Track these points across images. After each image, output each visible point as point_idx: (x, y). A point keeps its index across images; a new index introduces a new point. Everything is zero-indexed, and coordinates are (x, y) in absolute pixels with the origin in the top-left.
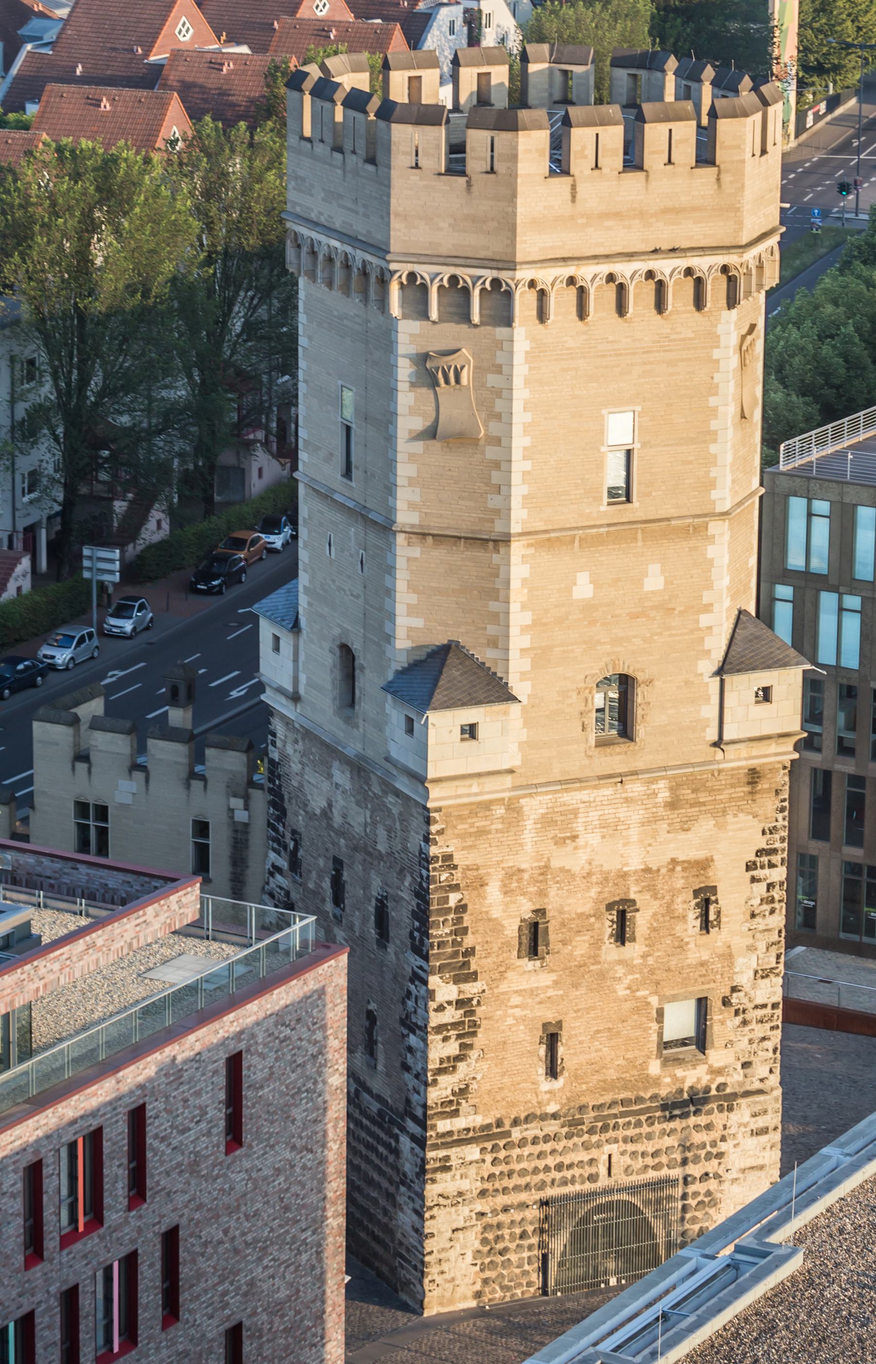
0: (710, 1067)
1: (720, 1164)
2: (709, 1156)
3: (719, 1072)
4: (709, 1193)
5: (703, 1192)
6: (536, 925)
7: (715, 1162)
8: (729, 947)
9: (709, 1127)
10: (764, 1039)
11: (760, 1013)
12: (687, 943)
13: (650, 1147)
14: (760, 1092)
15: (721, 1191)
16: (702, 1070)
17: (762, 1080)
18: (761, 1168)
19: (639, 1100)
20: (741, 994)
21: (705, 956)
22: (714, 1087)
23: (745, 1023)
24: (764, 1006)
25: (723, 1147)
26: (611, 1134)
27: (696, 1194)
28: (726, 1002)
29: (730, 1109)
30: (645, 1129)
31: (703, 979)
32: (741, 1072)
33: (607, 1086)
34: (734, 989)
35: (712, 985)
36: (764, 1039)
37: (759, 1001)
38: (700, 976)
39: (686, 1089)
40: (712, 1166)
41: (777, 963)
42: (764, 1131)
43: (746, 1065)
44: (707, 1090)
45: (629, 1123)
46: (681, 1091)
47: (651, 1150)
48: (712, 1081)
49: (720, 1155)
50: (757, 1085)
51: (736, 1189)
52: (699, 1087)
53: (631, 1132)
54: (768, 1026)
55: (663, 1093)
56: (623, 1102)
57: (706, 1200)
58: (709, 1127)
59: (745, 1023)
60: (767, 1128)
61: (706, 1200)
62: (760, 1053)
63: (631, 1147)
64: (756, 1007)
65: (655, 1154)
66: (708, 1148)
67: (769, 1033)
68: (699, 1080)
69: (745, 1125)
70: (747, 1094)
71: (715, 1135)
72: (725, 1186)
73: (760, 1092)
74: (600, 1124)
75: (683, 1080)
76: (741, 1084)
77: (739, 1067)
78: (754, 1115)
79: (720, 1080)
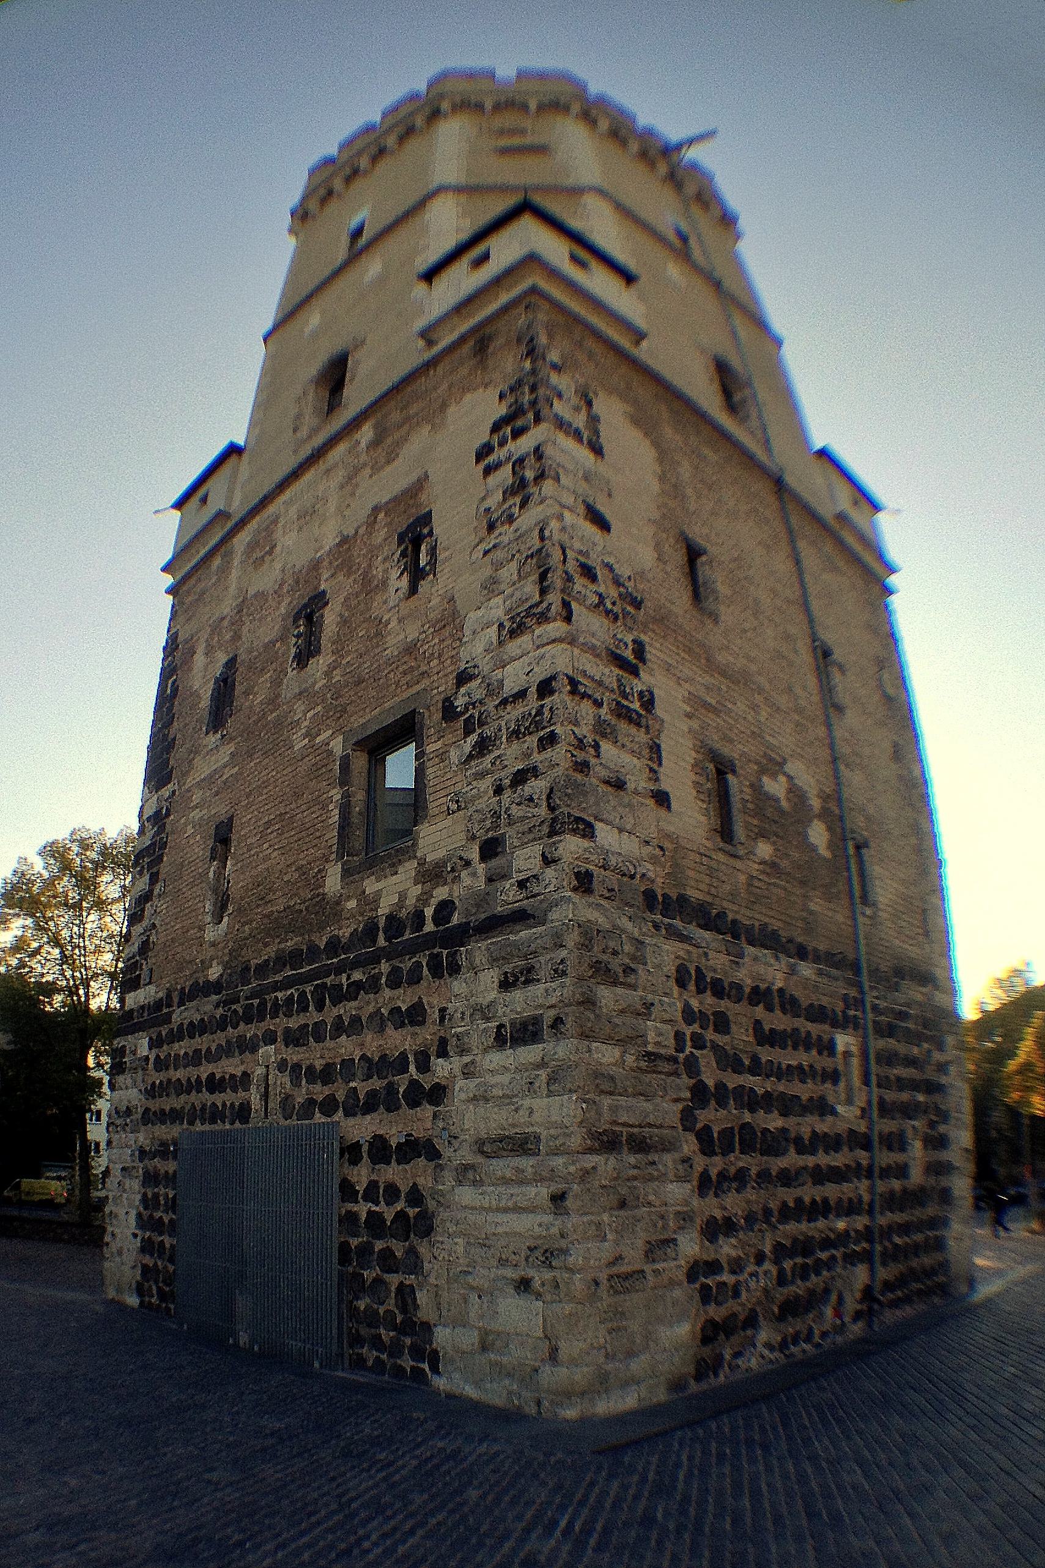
0: (422, 863)
1: (435, 1116)
2: (417, 1095)
3: (432, 875)
4: (415, 1196)
5: (404, 1188)
6: (225, 681)
7: (428, 1110)
8: (452, 599)
9: (415, 1015)
10: (520, 778)
11: (515, 712)
12: (388, 623)
13: (315, 1055)
14: (521, 917)
15: (435, 1193)
16: (408, 869)
17: (522, 884)
18: (522, 1144)
19: (313, 952)
20: (474, 684)
21: (412, 632)
22: (429, 912)
23: (483, 747)
24: (522, 694)
25: (442, 1068)
26: (269, 1024)
27: (392, 1193)
28: (449, 712)
29: (455, 969)
30: (313, 1016)
31: (408, 677)
32: (481, 868)
33: (275, 927)
34: (463, 678)
35: (425, 683)
36: (520, 778)
37: (510, 687)
38: (405, 673)
39: (382, 923)
40: (420, 1121)
41: (543, 592)
42: (525, 1032)
43: (490, 849)
44: (418, 917)
45: (290, 998)
46: (371, 930)
47: (319, 1064)
48: (424, 899)
49: (438, 1094)
50: (508, 896)
51: (466, 1195)
52: (403, 914)
53: (293, 1023)
54: (532, 741)
55: (345, 933)
56: (294, 958)
57: (412, 1212)
58: (415, 1015)
59: (483, 747)
60: (536, 1020)
61: (412, 1212)
62: (515, 811)
63: (294, 1055)
64: (504, 702)
65: (326, 1075)
66: (412, 1068)
67: (537, 758)
68: (403, 896)
69: (484, 1012)
70: (493, 924)
71: (427, 1034)
72: (449, 1178)
73: (521, 917)
74: (256, 1002)
75: (374, 902)
76: (482, 900)
77: (474, 854)
78: (506, 984)
79: (441, 893)
